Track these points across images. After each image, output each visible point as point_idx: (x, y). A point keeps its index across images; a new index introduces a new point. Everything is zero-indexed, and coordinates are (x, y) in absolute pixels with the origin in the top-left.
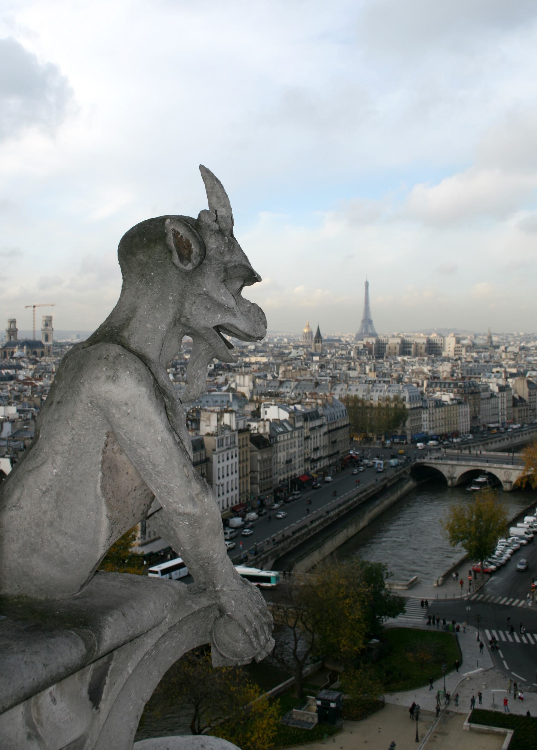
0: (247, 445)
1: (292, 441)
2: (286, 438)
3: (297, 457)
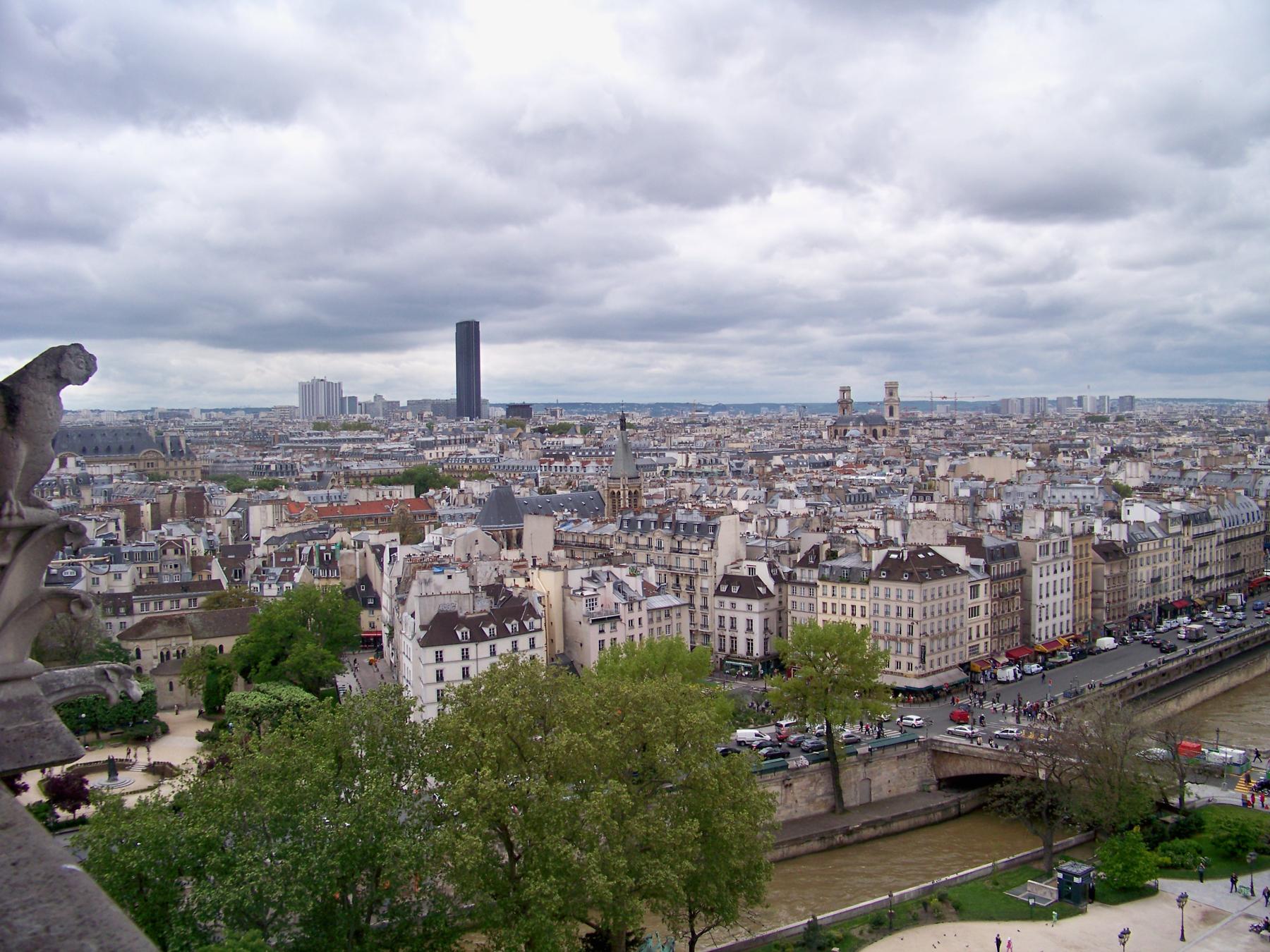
0: (1087, 555)
1: (1163, 552)
2: (1151, 547)
3: (1170, 574)
